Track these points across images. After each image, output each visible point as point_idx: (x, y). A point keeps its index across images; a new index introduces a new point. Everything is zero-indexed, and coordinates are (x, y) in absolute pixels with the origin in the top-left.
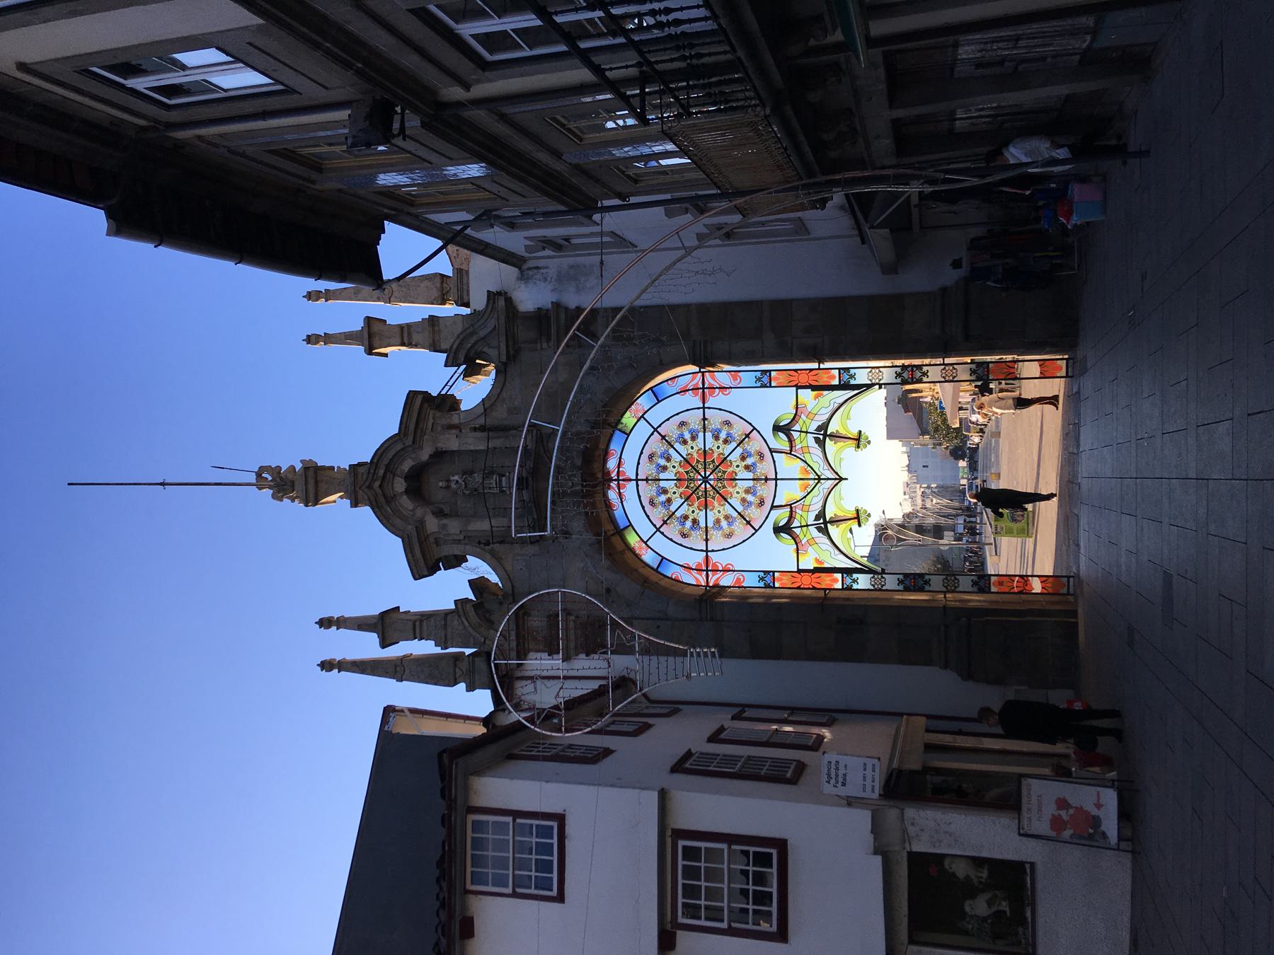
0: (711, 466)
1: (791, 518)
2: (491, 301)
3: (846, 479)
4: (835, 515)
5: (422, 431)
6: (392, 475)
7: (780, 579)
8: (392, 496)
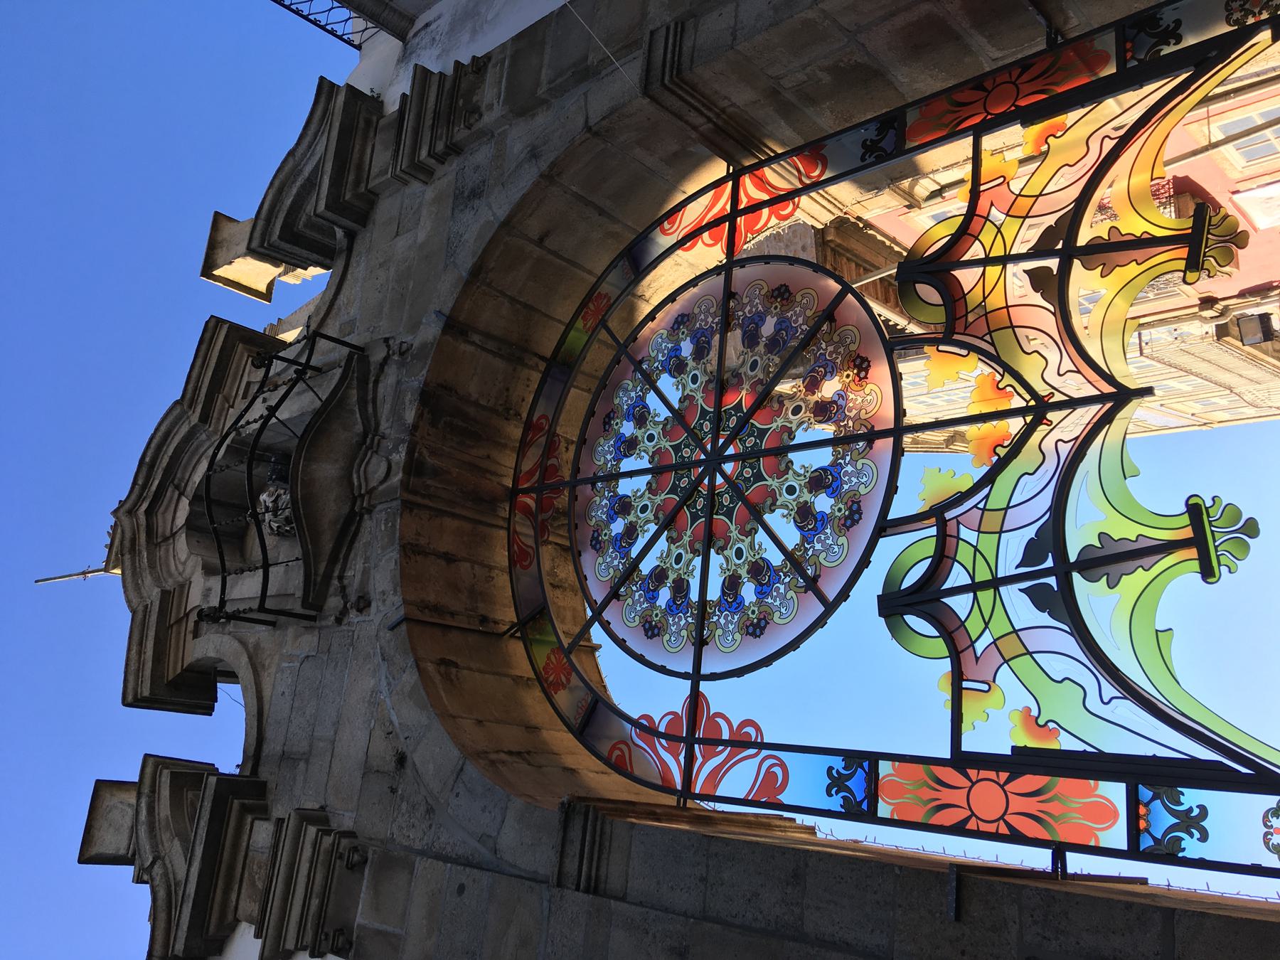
0: (750, 442)
1: (942, 559)
2: (323, 99)
3: (1148, 391)
4: (1101, 535)
5: (226, 399)
6: (177, 493)
7: (897, 791)
8: (168, 533)
